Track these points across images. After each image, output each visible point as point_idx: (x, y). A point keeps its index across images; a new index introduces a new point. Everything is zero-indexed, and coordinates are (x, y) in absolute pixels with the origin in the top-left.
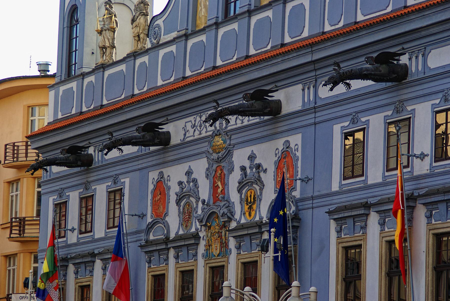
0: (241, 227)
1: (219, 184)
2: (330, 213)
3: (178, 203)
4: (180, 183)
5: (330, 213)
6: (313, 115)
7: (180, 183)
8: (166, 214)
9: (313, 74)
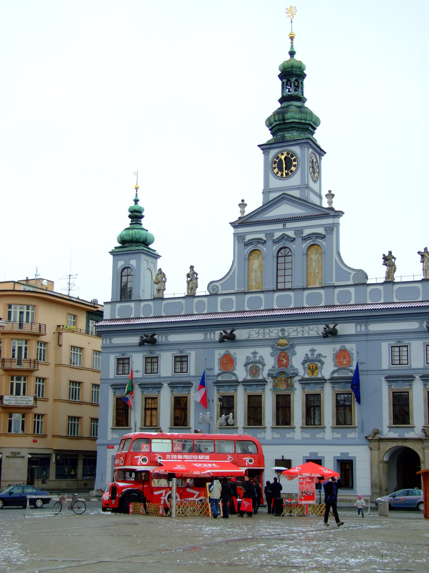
1: (284, 359)
2: (385, 378)
3: (246, 365)
4: (248, 357)
5: (385, 378)
6: (366, 337)
7: (248, 357)
8: (234, 370)
9: (366, 320)
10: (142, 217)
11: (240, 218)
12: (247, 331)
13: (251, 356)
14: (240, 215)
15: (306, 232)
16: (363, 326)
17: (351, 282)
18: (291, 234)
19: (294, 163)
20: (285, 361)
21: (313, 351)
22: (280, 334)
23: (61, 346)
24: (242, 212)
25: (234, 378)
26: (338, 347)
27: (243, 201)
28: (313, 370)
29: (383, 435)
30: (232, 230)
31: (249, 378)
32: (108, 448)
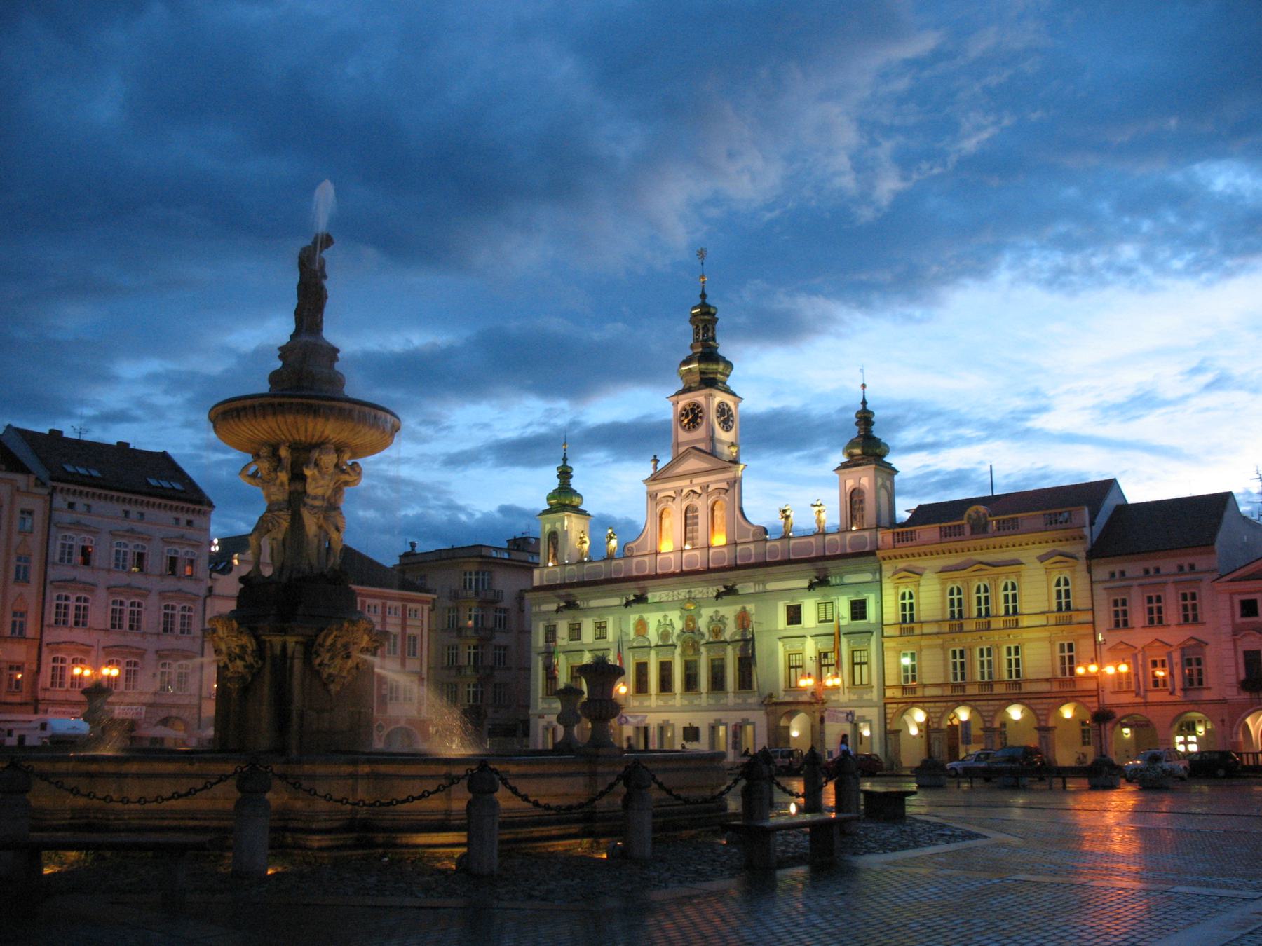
0: (708, 643)
10: (571, 477)
11: (652, 475)
12: (658, 594)
13: (662, 620)
14: (652, 471)
15: (712, 487)
16: (761, 585)
17: (751, 539)
18: (698, 490)
19: (700, 415)
20: (692, 626)
21: (717, 612)
22: (688, 596)
23: (523, 611)
24: (655, 467)
25: (647, 644)
26: (739, 608)
27: (655, 456)
28: (717, 632)
29: (778, 698)
30: (644, 488)
31: (660, 643)
32: (540, 717)
